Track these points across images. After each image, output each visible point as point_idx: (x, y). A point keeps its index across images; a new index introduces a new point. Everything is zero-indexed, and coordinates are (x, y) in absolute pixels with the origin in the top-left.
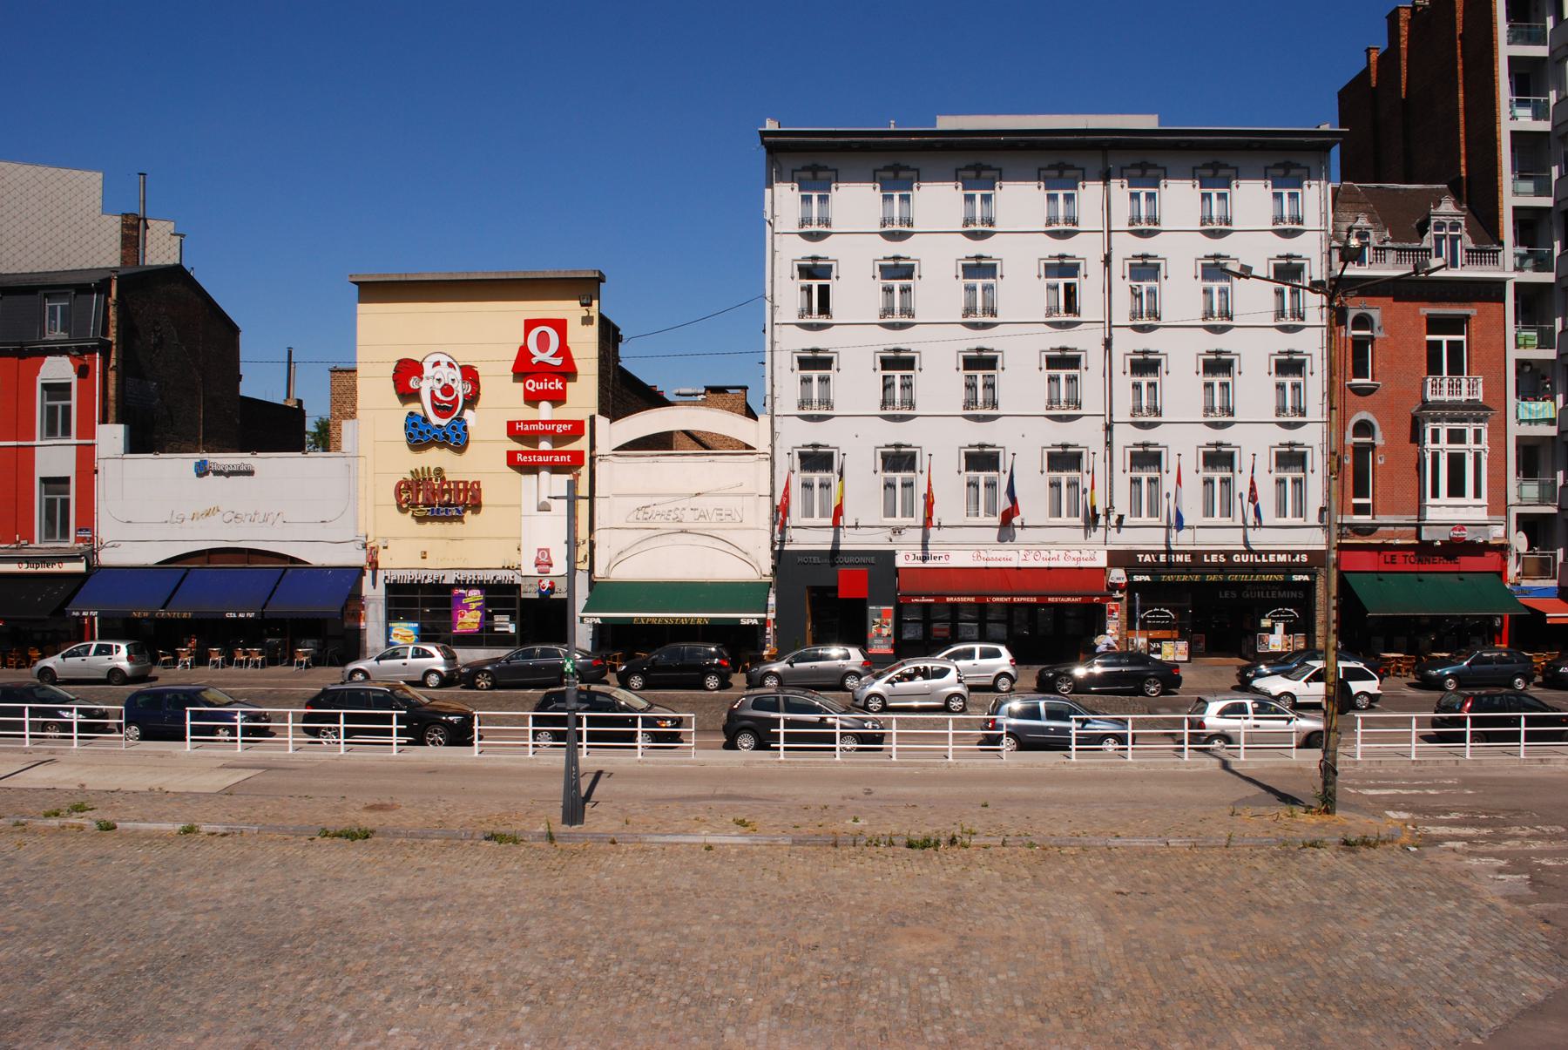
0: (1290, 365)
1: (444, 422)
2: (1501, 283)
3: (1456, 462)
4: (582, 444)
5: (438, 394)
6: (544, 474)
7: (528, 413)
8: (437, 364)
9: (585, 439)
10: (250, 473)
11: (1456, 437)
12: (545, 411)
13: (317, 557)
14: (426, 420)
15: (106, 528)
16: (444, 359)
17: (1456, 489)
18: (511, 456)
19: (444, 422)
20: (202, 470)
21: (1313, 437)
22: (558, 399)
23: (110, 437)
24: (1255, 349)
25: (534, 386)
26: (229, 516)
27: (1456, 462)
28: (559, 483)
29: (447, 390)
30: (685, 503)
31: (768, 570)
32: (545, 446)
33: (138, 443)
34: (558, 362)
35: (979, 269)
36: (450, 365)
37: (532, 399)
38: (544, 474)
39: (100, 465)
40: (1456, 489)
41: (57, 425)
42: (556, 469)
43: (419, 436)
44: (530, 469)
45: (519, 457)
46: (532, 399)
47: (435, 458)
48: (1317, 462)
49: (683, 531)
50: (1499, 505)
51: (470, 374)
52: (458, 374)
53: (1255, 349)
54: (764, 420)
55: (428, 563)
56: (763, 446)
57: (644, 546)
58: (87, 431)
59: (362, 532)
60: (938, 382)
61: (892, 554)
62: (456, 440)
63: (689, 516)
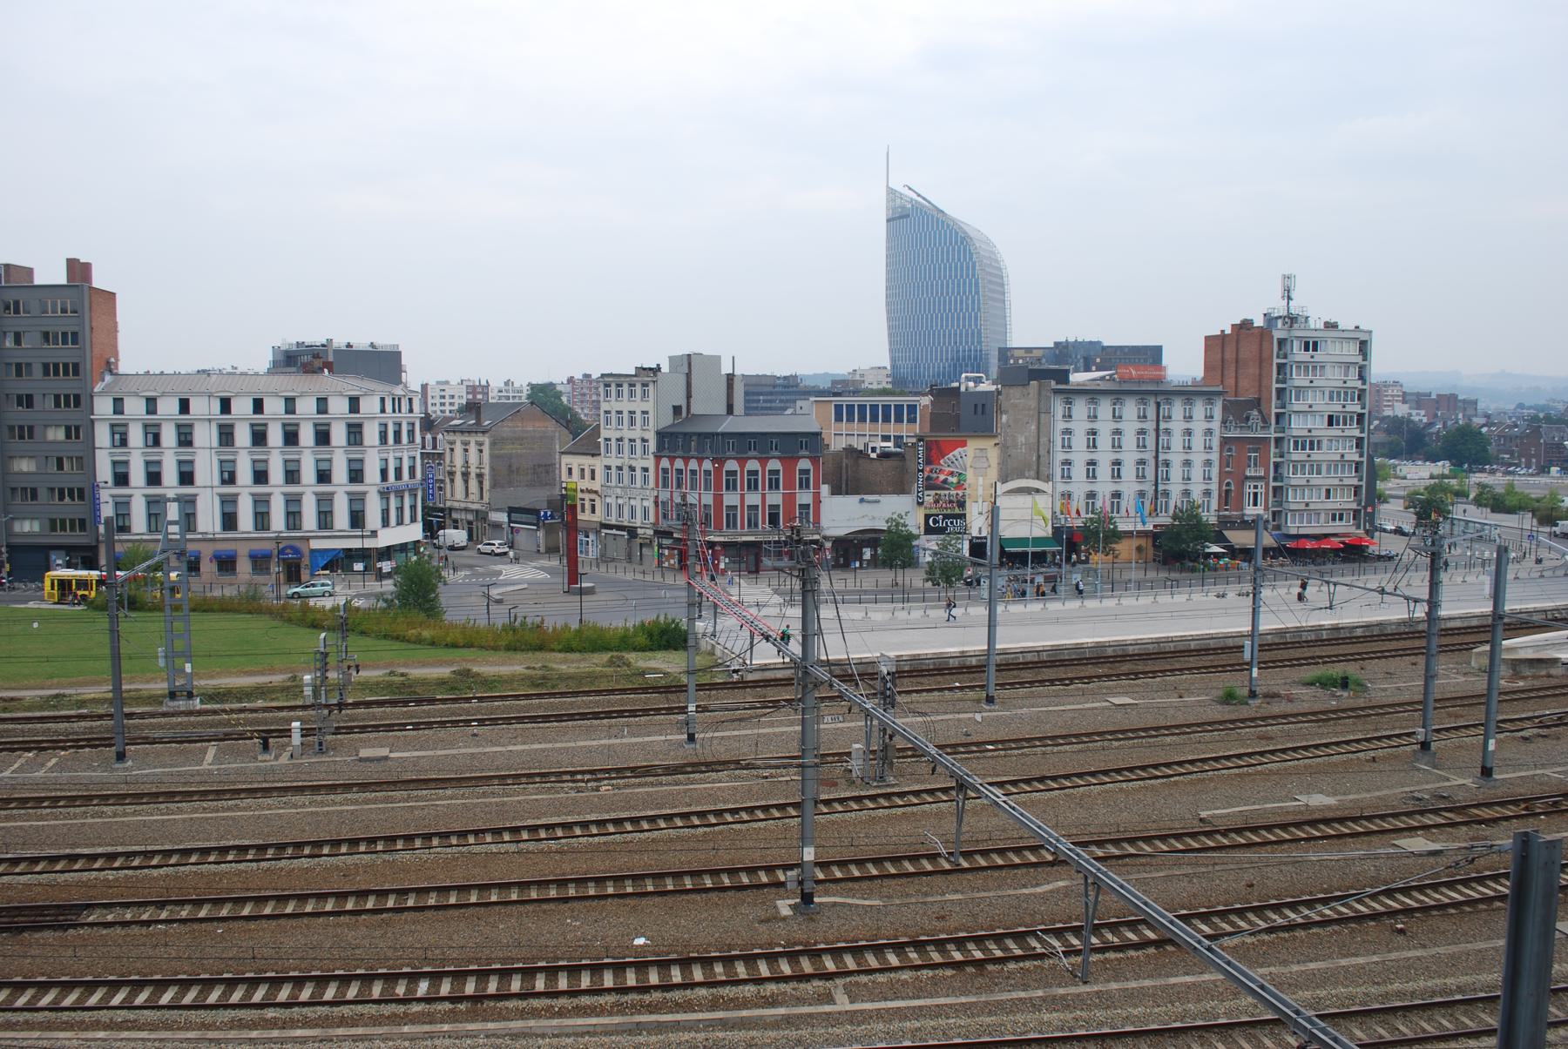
0: (1208, 463)
3: (1255, 494)
15: (824, 522)
17: (1255, 504)
20: (862, 501)
21: (1214, 487)
23: (825, 489)
24: (1198, 458)
27: (1255, 494)
33: (836, 491)
35: (1118, 432)
40: (1255, 504)
41: (804, 484)
48: (1215, 495)
50: (1266, 508)
53: (1198, 458)
58: (817, 486)
60: (1104, 471)
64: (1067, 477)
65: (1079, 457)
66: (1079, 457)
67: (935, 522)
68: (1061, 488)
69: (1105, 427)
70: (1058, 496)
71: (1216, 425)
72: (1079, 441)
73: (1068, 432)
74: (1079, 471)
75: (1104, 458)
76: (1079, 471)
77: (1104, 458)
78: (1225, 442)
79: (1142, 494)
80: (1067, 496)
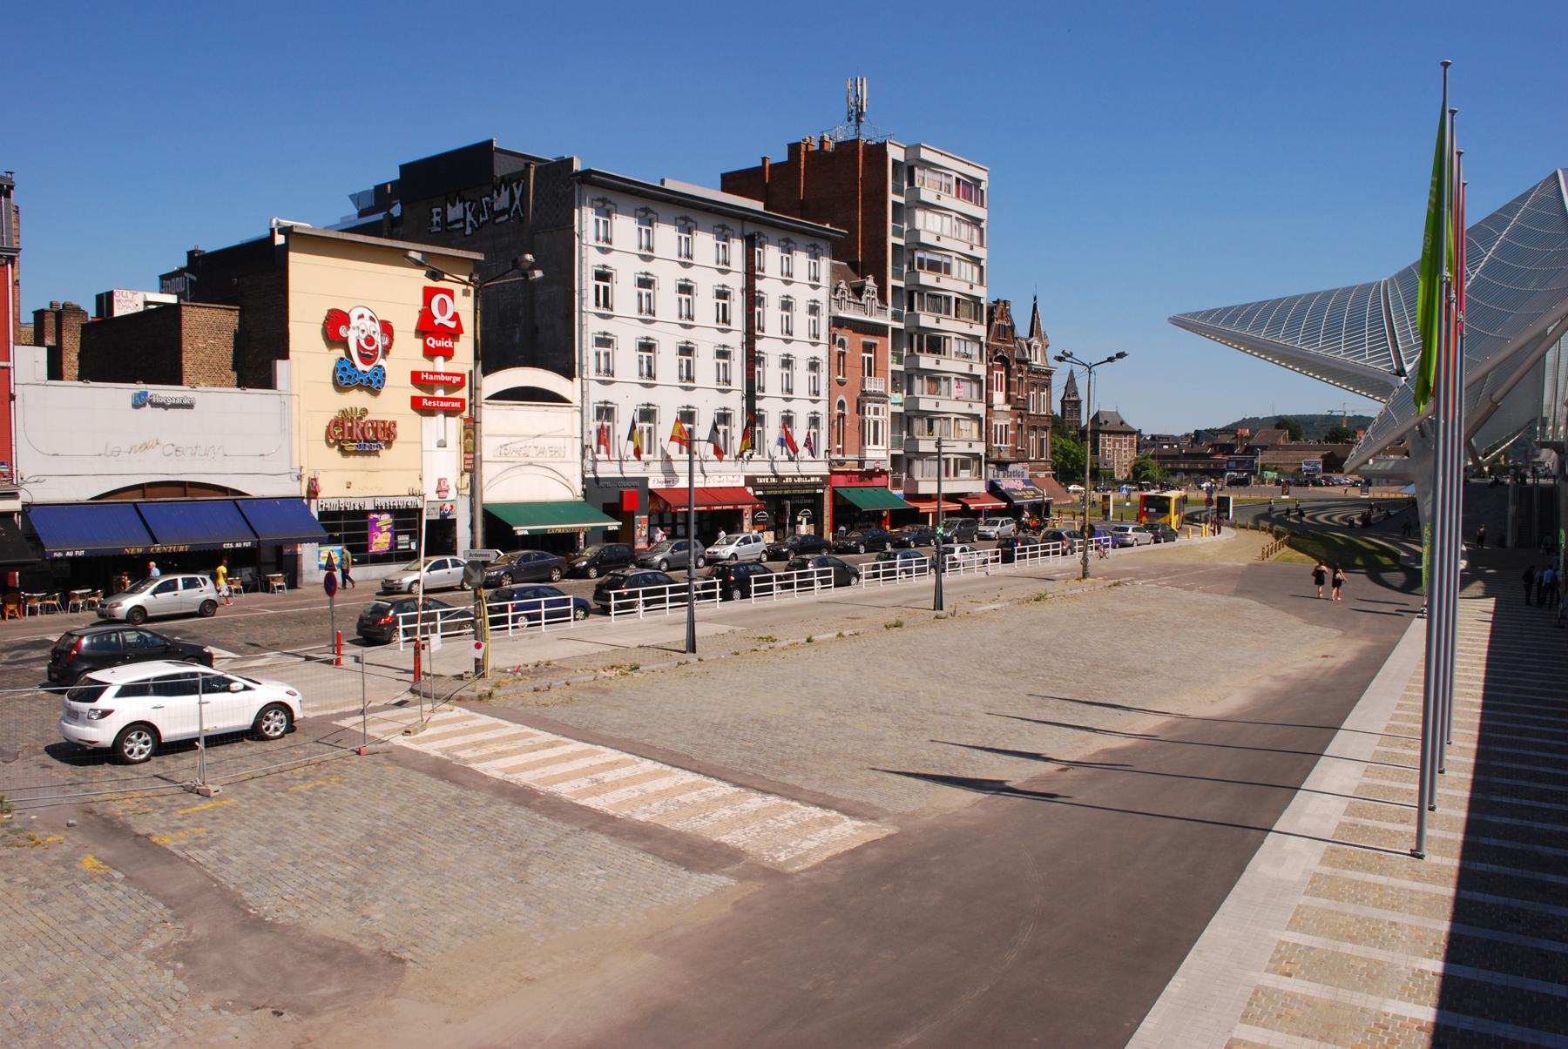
1: (367, 368)
2: (886, 327)
4: (463, 393)
5: (363, 343)
6: (441, 416)
7: (424, 365)
8: (361, 316)
9: (466, 388)
10: (190, 406)
11: (876, 412)
12: (440, 364)
13: (256, 488)
14: (353, 366)
16: (367, 314)
17: (876, 442)
18: (416, 403)
19: (367, 368)
20: (139, 402)
21: (822, 408)
22: (448, 354)
25: (434, 343)
26: (170, 449)
28: (455, 424)
29: (370, 341)
30: (529, 443)
31: (579, 492)
32: (440, 393)
34: (452, 325)
36: (372, 319)
37: (430, 353)
38: (441, 416)
39: (17, 391)
42: (449, 412)
43: (344, 380)
44: (429, 412)
45: (425, 402)
46: (430, 353)
47: (356, 399)
49: (530, 464)
51: (387, 328)
52: (377, 327)
54: (577, 380)
55: (352, 492)
56: (576, 401)
57: (510, 473)
59: (296, 465)
60: (667, 363)
61: (646, 479)
62: (373, 385)
63: (533, 452)
64: (607, 375)
65: (627, 333)
66: (627, 333)
68: (598, 394)
69: (667, 275)
70: (591, 412)
71: (822, 295)
72: (625, 294)
73: (603, 276)
74: (626, 360)
75: (668, 339)
76: (626, 360)
77: (668, 339)
78: (837, 322)
79: (724, 417)
80: (606, 412)
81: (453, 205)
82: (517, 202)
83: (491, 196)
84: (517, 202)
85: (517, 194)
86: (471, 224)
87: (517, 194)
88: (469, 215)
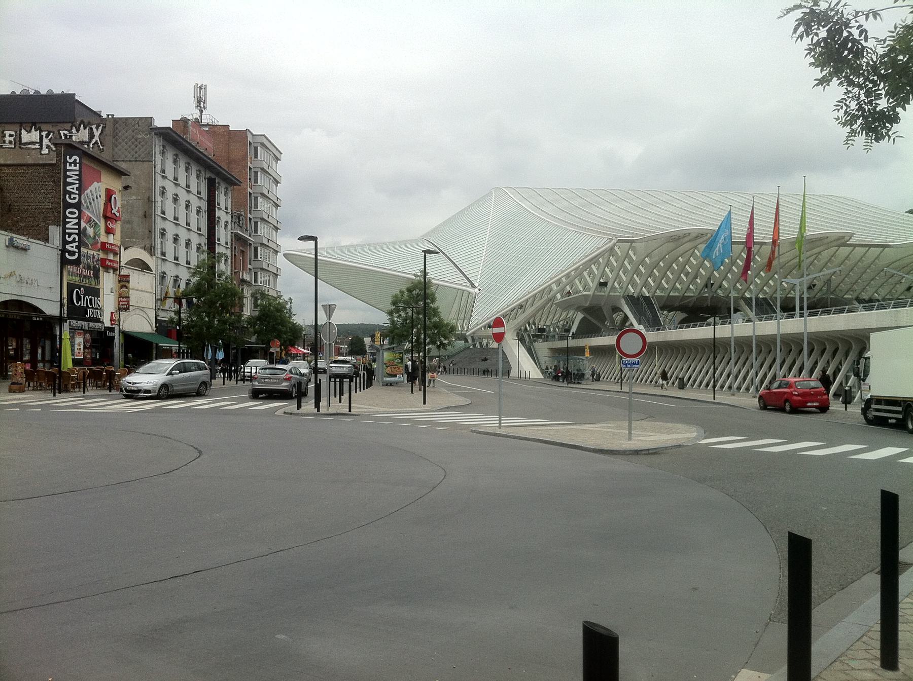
20: (11, 245)
67: (79, 299)
81: (29, 132)
82: (96, 138)
83: (70, 131)
84: (96, 138)
85: (97, 133)
86: (48, 147)
87: (97, 133)
88: (46, 141)
